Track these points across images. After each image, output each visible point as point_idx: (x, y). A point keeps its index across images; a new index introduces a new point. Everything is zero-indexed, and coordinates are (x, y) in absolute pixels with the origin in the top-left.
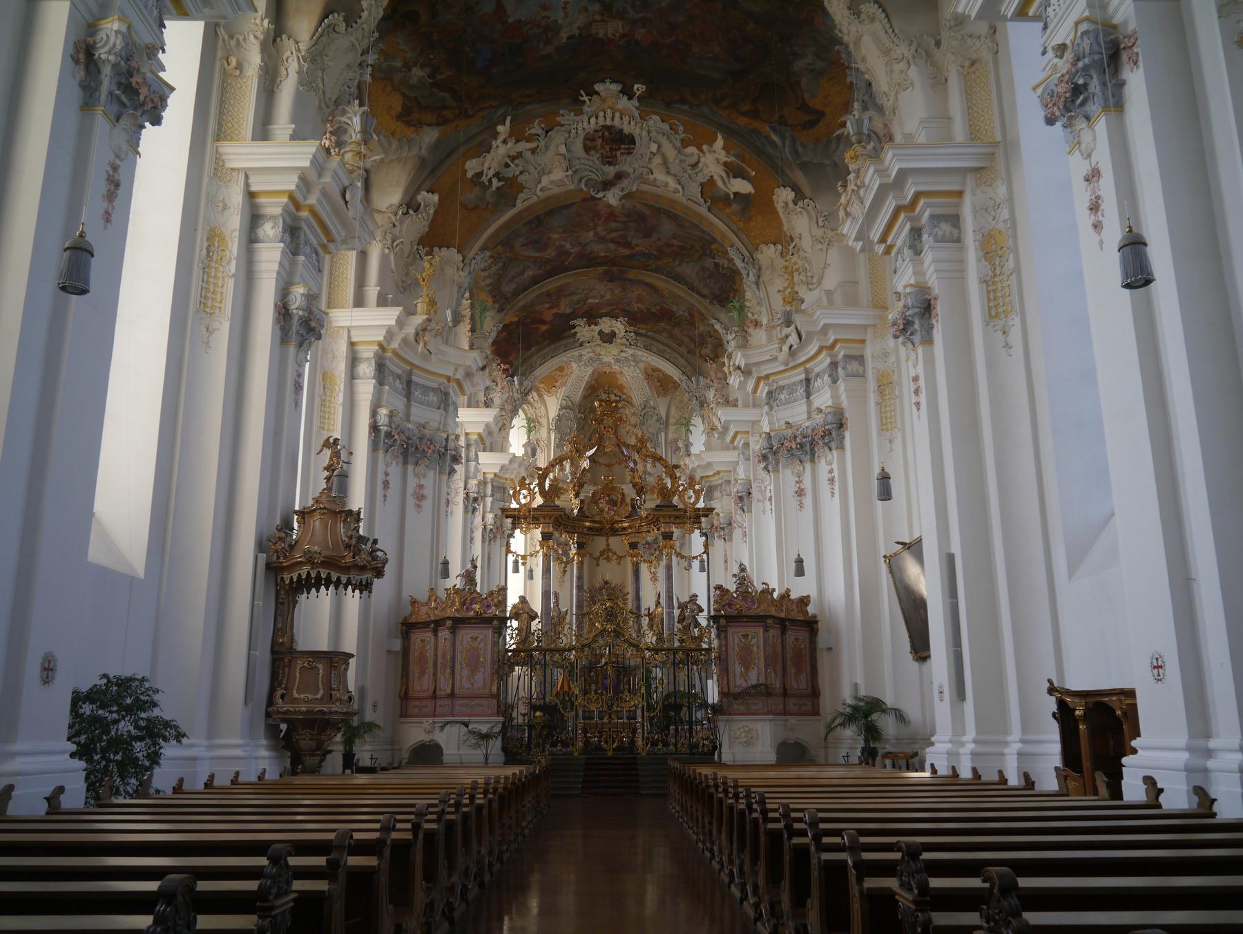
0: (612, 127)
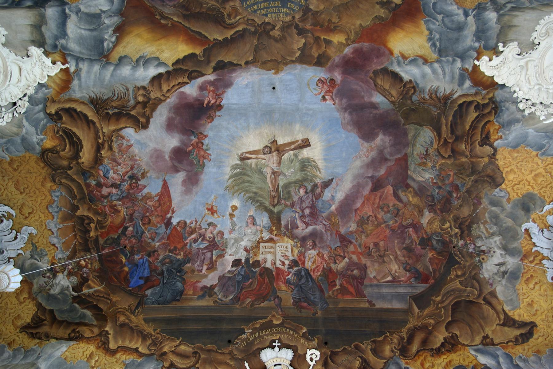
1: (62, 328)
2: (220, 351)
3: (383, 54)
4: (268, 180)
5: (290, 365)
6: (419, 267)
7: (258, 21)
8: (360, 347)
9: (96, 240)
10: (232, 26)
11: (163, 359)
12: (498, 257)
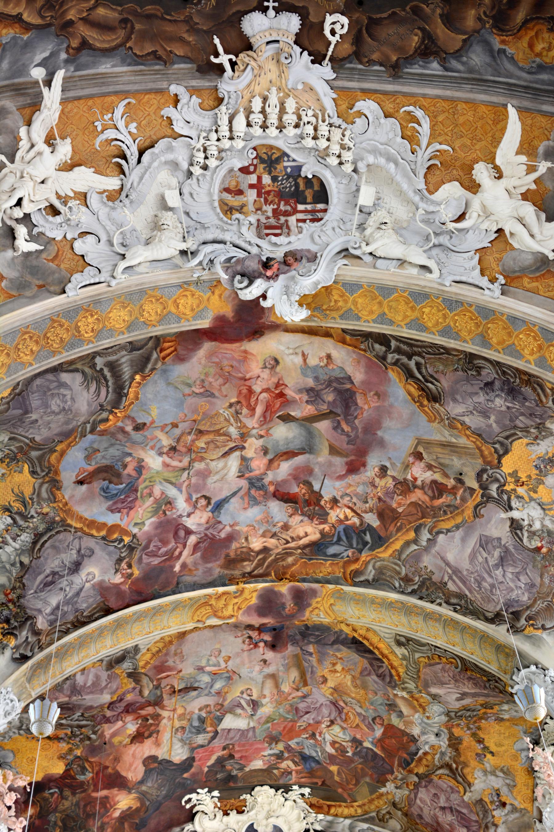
2: (168, 17)
5: (296, 43)
8: (422, 10)
11: (68, 33)
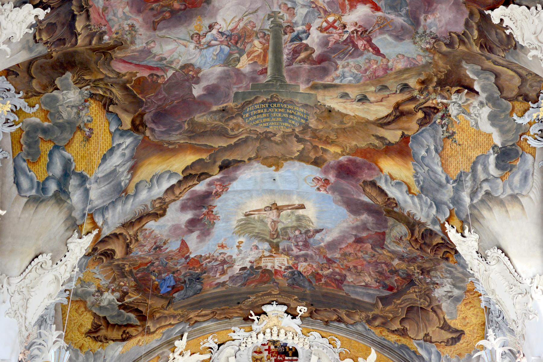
0: (278, 341)
1: (115, 330)
3: (374, 169)
4: (269, 225)
6: (387, 282)
7: (260, 131)
9: (131, 271)
10: (235, 136)
12: (448, 288)
